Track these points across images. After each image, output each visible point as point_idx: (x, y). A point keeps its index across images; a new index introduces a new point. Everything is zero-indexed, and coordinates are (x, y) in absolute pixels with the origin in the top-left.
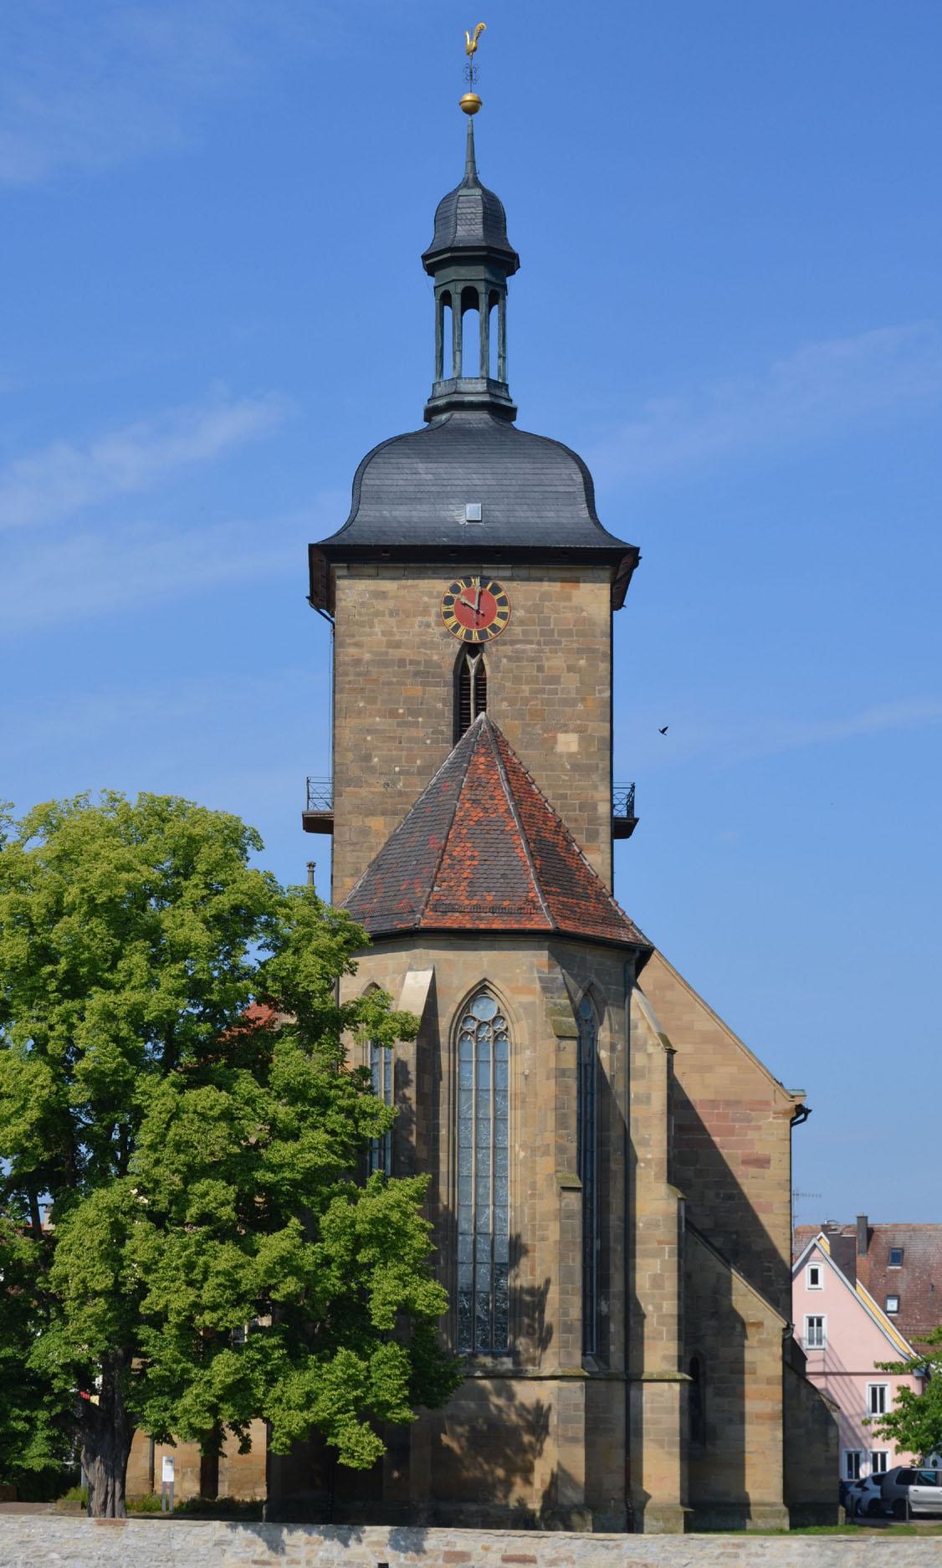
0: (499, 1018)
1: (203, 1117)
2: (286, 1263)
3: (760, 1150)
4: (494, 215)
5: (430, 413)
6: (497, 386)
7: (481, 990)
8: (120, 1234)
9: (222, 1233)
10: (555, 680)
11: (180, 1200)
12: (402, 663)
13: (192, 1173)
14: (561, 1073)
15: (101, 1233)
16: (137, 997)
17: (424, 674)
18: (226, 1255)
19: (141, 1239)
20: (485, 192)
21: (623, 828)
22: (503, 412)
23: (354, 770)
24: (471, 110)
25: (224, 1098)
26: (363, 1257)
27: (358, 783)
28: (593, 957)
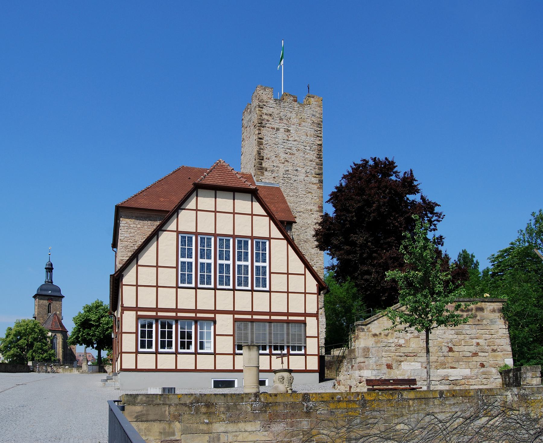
0: (57, 337)
1: (39, 345)
2: (46, 356)
3: (74, 347)
4: (52, 265)
5: (45, 282)
6: (52, 280)
7: (55, 335)
8: (32, 354)
9: (40, 354)
10: (57, 307)
11: (37, 351)
12: (43, 305)
13: (38, 349)
14: (62, 342)
15: (31, 353)
16: (34, 336)
17: (46, 306)
18: (41, 356)
19: (34, 354)
20: (51, 263)
21: (62, 319)
22: (52, 282)
23: (39, 314)
24: (50, 254)
25: (41, 344)
26: (51, 356)
27: (39, 315)
28: (64, 332)
